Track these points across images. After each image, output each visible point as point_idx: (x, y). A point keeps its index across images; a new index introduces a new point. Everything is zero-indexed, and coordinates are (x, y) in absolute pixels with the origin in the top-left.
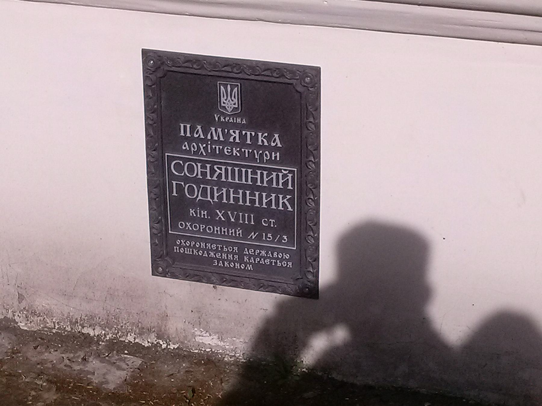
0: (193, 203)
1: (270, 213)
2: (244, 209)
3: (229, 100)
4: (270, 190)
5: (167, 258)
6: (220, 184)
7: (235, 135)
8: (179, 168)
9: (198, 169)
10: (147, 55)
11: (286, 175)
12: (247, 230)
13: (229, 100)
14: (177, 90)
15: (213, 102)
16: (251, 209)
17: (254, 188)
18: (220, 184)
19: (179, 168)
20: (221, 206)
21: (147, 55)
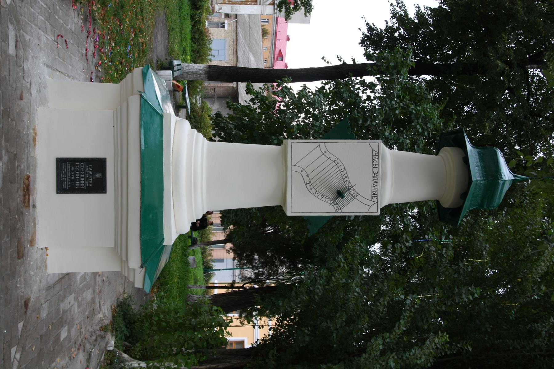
0: (75, 168)
1: (75, 183)
2: (75, 178)
3: (98, 176)
4: (80, 184)
5: (61, 163)
6: (80, 173)
7: (91, 177)
8: (82, 165)
9: (83, 169)
10: (105, 159)
11: (83, 187)
12: (70, 179)
13: (98, 176)
14: (98, 165)
15: (97, 172)
16: (75, 180)
17: (80, 180)
18: (80, 173)
19: (82, 165)
20: (75, 173)
21: (105, 159)
